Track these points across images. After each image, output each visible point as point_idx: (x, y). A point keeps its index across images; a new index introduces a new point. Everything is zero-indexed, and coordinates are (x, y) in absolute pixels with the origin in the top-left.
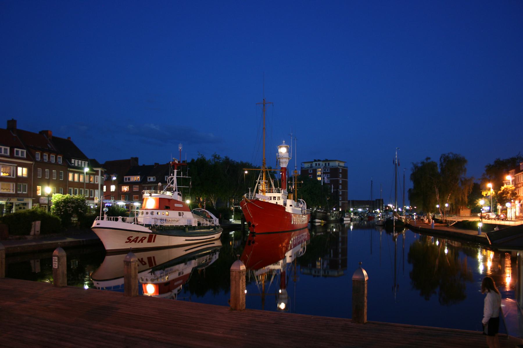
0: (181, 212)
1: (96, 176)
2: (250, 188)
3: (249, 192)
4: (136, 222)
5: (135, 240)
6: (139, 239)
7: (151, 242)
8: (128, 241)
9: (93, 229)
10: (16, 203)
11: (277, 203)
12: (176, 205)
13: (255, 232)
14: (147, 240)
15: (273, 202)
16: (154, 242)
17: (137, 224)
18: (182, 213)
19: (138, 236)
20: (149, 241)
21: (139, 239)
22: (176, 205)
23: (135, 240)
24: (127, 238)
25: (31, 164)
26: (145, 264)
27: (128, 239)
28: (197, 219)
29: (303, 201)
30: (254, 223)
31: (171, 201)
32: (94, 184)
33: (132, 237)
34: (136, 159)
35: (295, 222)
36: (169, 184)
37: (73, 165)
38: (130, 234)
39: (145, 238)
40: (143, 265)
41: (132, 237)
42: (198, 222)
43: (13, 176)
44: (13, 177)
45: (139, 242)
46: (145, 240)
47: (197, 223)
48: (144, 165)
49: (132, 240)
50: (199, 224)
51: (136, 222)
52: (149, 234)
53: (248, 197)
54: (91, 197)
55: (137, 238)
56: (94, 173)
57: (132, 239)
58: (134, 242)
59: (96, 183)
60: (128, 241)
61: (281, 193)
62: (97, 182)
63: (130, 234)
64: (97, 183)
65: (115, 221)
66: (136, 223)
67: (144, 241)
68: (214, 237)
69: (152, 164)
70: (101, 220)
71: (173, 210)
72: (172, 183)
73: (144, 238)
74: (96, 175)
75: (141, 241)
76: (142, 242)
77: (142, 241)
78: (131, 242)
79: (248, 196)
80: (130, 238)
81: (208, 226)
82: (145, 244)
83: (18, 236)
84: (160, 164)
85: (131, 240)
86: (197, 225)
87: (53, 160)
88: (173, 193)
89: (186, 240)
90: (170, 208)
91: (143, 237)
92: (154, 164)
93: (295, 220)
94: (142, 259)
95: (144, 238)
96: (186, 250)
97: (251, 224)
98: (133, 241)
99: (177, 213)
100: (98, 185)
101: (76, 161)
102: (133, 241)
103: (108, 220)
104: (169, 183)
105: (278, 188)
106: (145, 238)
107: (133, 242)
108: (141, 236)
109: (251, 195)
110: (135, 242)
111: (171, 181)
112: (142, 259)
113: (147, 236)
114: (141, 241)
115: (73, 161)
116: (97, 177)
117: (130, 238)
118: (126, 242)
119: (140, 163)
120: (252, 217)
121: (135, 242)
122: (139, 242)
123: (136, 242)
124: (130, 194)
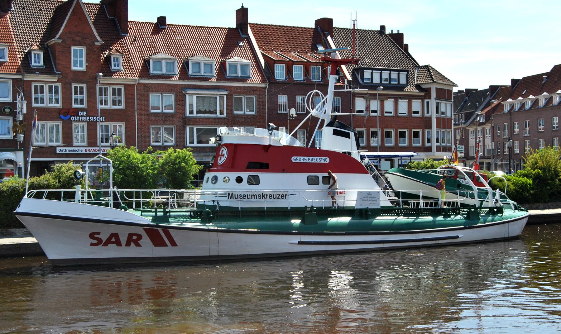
0: (320, 175)
1: (426, 101)
5: (113, 240)
8: (95, 242)
12: (296, 159)
21: (123, 239)
25: (263, 87)
27: (92, 236)
33: (99, 233)
38: (96, 228)
39: (140, 237)
41: (99, 233)
43: (221, 113)
44: (222, 116)
49: (104, 241)
56: (423, 94)
57: (104, 237)
59: (426, 114)
62: (428, 112)
63: (96, 228)
68: (457, 237)
70: (81, 197)
74: (426, 98)
75: (132, 244)
78: (106, 244)
87: (376, 75)
89: (300, 243)
90: (268, 168)
91: (130, 235)
99: (304, 176)
100: (430, 118)
101: (374, 74)
114: (132, 244)
116: (428, 103)
118: (92, 244)
122: (128, 244)
123: (119, 243)
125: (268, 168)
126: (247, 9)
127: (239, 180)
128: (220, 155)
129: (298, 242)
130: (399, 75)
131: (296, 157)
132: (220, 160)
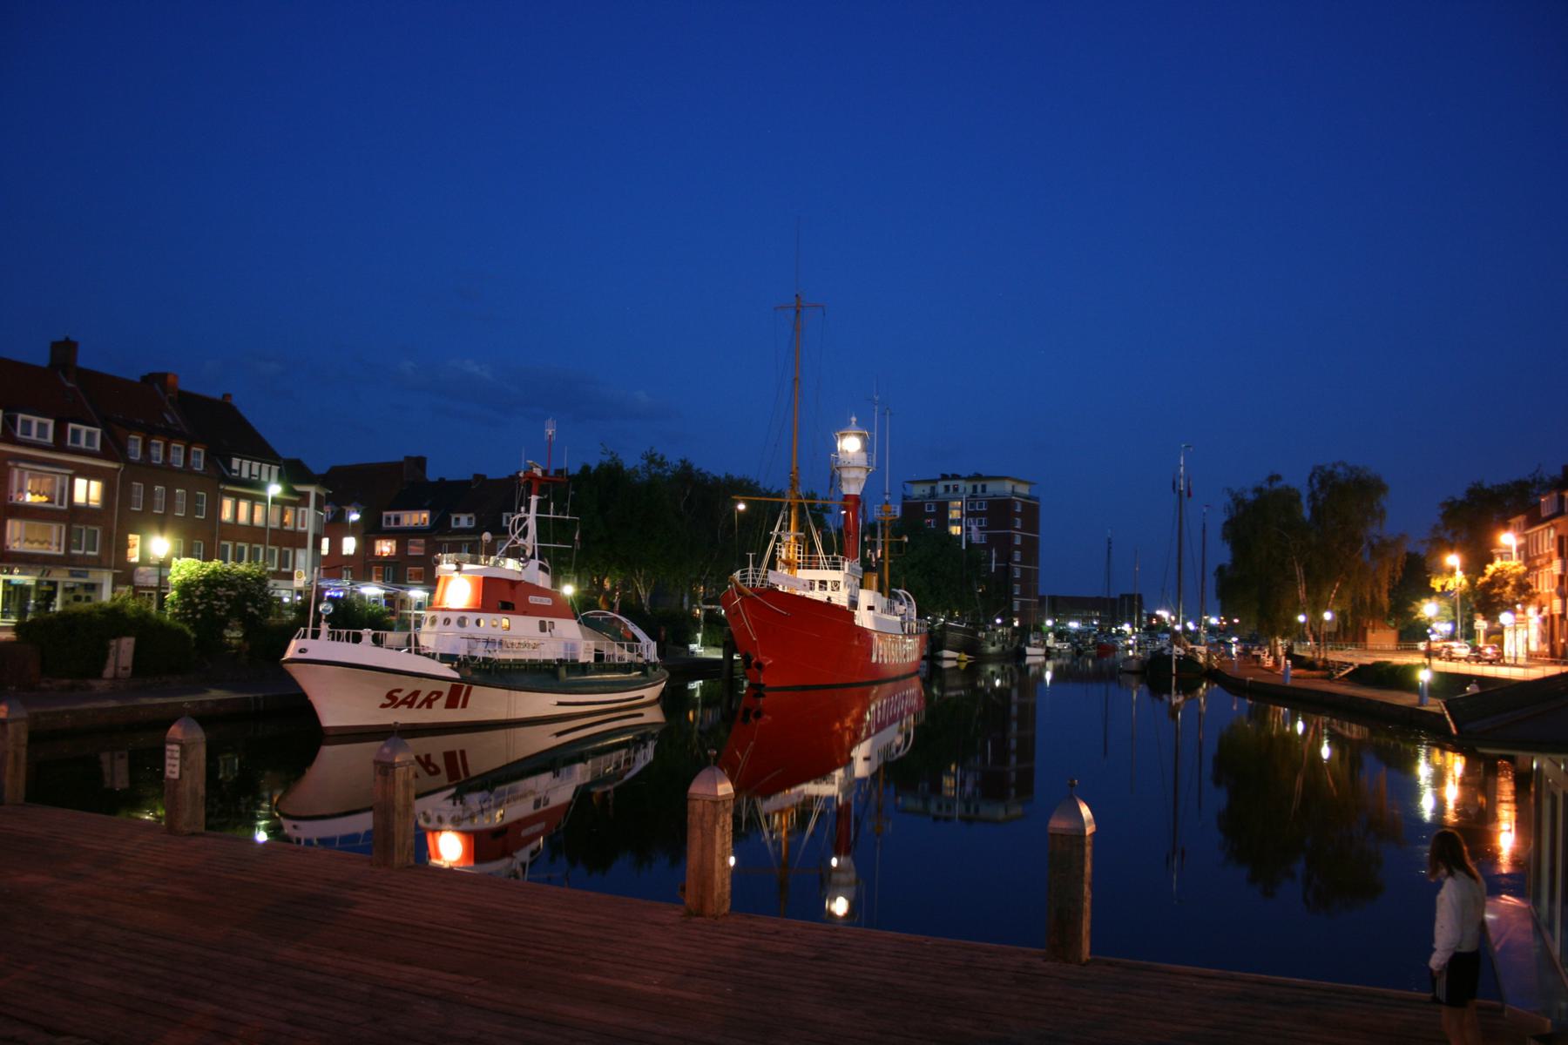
0: (547, 620)
2: (751, 555)
3: (748, 567)
4: (413, 647)
6: (421, 698)
7: (455, 706)
8: (388, 701)
9: (285, 665)
10: (64, 582)
11: (829, 599)
12: (533, 600)
13: (763, 685)
14: (443, 700)
15: (818, 595)
16: (464, 706)
17: (417, 652)
18: (550, 622)
19: (417, 689)
20: (451, 704)
21: (421, 698)
22: (533, 600)
23: (409, 700)
24: (385, 694)
25: (114, 469)
26: (437, 771)
27: (390, 695)
28: (592, 644)
29: (906, 596)
30: (762, 658)
31: (518, 588)
32: (294, 533)
33: (399, 691)
34: (420, 463)
35: (882, 656)
36: (513, 538)
37: (237, 475)
39: (439, 694)
40: (431, 774)
41: (399, 691)
42: (596, 650)
43: (61, 503)
44: (61, 507)
46: (439, 701)
47: (594, 652)
48: (442, 480)
49: (399, 700)
50: (599, 657)
51: (413, 647)
52: (449, 684)
53: (745, 581)
54: (284, 570)
55: (416, 694)
56: (297, 499)
57: (401, 696)
58: (406, 706)
59: (300, 528)
60: (388, 701)
61: (843, 569)
62: (303, 525)
64: (303, 529)
65: (353, 642)
66: (413, 651)
67: (434, 703)
68: (642, 697)
69: (465, 478)
71: (525, 613)
72: (524, 534)
73: (434, 696)
75: (425, 705)
76: (430, 706)
77: (429, 702)
78: (396, 707)
79: (746, 576)
80: (395, 694)
81: (626, 665)
82: (439, 714)
83: (67, 682)
84: (488, 477)
85: (396, 698)
86: (592, 661)
87: (178, 459)
88: (525, 564)
89: (560, 704)
91: (433, 693)
92: (471, 477)
93: (883, 650)
94: (428, 757)
95: (434, 696)
96: (559, 734)
97: (751, 660)
98: (404, 702)
99: (533, 622)
100: (305, 534)
102: (404, 702)
103: (333, 639)
104: (514, 533)
105: (835, 555)
106: (439, 694)
107: (404, 707)
108: (426, 688)
109: (753, 576)
110: (408, 707)
111: (521, 529)
112: (428, 757)
113: (446, 688)
114: (425, 705)
115: (235, 463)
116: (303, 512)
117: (395, 694)
118: (383, 706)
119: (432, 475)
120: (754, 639)
121: (408, 707)
122: (419, 707)
123: (410, 705)
124: (398, 563)
126: (75, 345)
129: (556, 703)
130: (241, 463)
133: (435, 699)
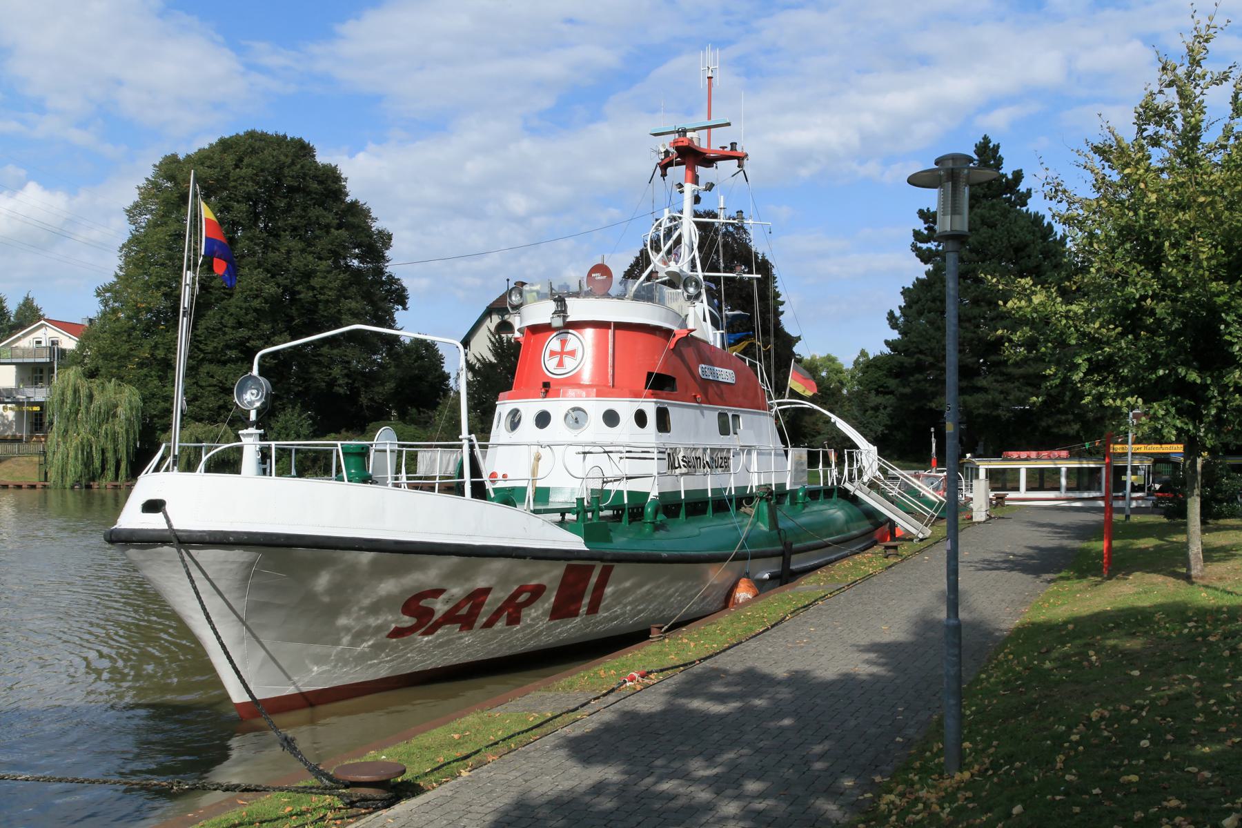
8: (408, 621)
17: (479, 491)
20: (562, 610)
23: (464, 611)
33: (436, 593)
45: (489, 624)
57: (440, 607)
60: (408, 621)
65: (278, 475)
67: (524, 612)
76: (514, 620)
77: (512, 610)
95: (523, 598)
98: (449, 618)
111: (670, 242)
113: (551, 576)
123: (467, 622)
125: (673, 388)
127: (641, 418)
128: (553, 353)
131: (703, 366)
132: (560, 364)
133: (528, 603)
